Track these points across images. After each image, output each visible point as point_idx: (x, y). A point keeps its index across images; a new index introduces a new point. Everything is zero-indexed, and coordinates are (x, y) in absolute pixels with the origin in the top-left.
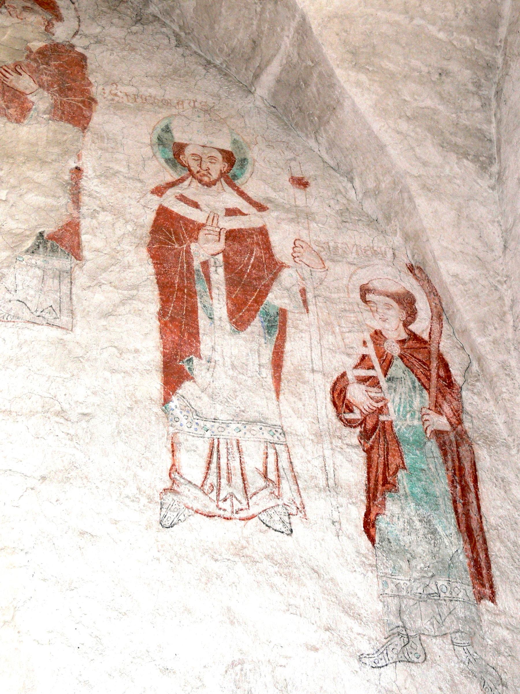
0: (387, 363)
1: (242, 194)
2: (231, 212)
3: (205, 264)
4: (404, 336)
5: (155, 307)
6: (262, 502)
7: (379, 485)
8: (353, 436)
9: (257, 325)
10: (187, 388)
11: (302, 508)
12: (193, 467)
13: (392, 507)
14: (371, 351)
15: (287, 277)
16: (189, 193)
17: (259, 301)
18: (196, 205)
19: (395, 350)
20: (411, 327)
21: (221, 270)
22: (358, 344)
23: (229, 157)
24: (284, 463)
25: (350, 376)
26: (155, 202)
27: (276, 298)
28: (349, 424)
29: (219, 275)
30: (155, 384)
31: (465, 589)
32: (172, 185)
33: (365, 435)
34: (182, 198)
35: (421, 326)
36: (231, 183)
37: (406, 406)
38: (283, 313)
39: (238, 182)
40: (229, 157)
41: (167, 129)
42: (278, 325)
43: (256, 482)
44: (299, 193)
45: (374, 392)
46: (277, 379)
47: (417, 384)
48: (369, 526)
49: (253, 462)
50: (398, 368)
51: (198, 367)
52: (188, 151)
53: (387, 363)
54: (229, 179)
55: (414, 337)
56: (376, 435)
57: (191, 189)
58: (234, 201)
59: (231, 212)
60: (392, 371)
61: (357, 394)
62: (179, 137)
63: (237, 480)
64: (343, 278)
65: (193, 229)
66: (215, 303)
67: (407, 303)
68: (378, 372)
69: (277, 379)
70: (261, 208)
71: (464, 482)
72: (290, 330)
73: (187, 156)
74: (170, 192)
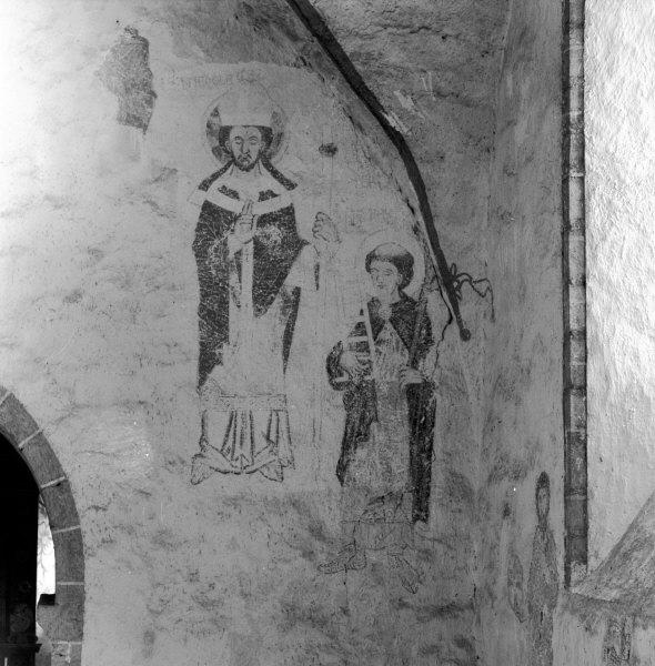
0: (377, 325)
1: (275, 173)
2: (264, 196)
3: (239, 253)
4: (398, 299)
5: (196, 303)
6: (264, 457)
7: (354, 436)
8: (339, 397)
9: (278, 301)
10: (217, 371)
11: (291, 462)
12: (216, 437)
13: (361, 453)
14: (366, 319)
15: (307, 254)
16: (230, 185)
17: (279, 283)
18: (235, 195)
19: (385, 312)
20: (404, 290)
21: (251, 258)
22: (354, 312)
23: (267, 134)
24: (283, 427)
25: (345, 345)
26: (203, 196)
27: (292, 281)
28: (337, 387)
29: (248, 265)
32: (215, 176)
33: (348, 398)
34: (224, 190)
35: (412, 290)
36: (268, 166)
37: (388, 366)
38: (297, 291)
39: (273, 161)
40: (267, 134)
41: (216, 113)
42: (293, 303)
43: (261, 442)
44: (326, 160)
46: (286, 355)
47: (401, 343)
48: (342, 468)
49: (260, 428)
50: (388, 333)
51: (225, 351)
52: (232, 135)
53: (377, 325)
54: (265, 159)
55: (405, 298)
57: (232, 179)
58: (269, 183)
59: (264, 196)
60: (382, 335)
61: (349, 360)
62: (226, 120)
63: (247, 441)
64: (350, 251)
65: (232, 218)
67: (404, 264)
68: (369, 338)
69: (286, 355)
70: (291, 186)
71: (421, 425)
72: (302, 310)
74: (217, 184)
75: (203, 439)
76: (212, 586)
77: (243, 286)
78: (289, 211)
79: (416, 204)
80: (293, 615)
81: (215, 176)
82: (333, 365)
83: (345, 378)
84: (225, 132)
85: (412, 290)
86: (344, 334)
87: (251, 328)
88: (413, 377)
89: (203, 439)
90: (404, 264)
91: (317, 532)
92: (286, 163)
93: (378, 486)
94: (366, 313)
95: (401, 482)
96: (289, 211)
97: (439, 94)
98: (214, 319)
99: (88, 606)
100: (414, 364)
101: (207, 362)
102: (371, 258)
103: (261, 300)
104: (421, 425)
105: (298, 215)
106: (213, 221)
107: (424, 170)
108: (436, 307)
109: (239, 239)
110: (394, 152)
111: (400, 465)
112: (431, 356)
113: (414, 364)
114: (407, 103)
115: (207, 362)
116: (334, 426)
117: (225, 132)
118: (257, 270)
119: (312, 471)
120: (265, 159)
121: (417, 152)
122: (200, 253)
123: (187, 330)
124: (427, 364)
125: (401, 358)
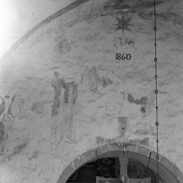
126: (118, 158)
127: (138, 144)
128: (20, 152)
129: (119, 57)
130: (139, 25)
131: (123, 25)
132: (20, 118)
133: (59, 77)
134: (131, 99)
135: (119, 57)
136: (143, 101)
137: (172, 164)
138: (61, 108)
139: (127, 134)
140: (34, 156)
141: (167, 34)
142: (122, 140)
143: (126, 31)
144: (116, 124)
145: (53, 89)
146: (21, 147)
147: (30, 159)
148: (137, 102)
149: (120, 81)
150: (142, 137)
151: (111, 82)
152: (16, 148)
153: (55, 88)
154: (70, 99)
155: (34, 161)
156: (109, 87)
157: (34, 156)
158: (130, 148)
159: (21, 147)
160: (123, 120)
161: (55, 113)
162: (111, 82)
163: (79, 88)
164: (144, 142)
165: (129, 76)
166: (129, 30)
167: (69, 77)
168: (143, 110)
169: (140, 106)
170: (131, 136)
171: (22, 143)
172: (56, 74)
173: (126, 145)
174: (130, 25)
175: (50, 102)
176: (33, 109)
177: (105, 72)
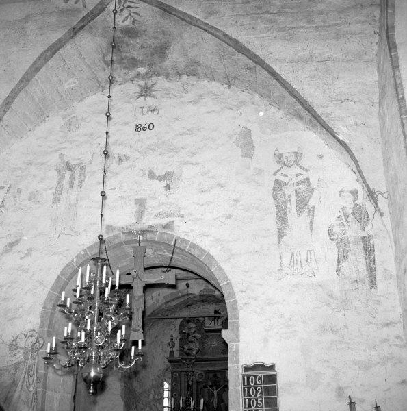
0: (347, 216)
1: (301, 167)
2: (297, 175)
5: (275, 214)
8: (334, 244)
9: (306, 211)
12: (286, 262)
14: (342, 214)
17: (306, 205)
18: (286, 176)
19: (349, 211)
20: (356, 202)
21: (294, 197)
23: (296, 155)
24: (313, 256)
25: (334, 224)
26: (274, 178)
27: (311, 203)
29: (294, 199)
30: (275, 239)
31: (368, 285)
32: (278, 171)
35: (359, 202)
37: (353, 231)
38: (313, 207)
39: (299, 163)
40: (296, 155)
42: (312, 211)
43: (304, 263)
44: (320, 161)
45: (342, 228)
46: (311, 230)
48: (338, 270)
49: (304, 257)
50: (351, 218)
51: (287, 231)
52: (284, 156)
54: (297, 163)
55: (357, 205)
56: (343, 243)
57: (285, 170)
58: (298, 170)
59: (297, 175)
60: (349, 219)
61: (337, 230)
63: (299, 263)
65: (286, 184)
66: (292, 207)
67: (355, 193)
69: (311, 230)
71: (369, 251)
72: (316, 213)
73: (284, 159)
74: (280, 172)
75: (281, 263)
76: (290, 319)
77: (292, 207)
78: (308, 179)
79: (355, 169)
80: (323, 329)
81: (278, 171)
82: (330, 232)
83: (336, 236)
84: (281, 155)
85: (359, 202)
86: (333, 220)
87: (297, 222)
88: (363, 234)
89: (281, 263)
90: (355, 193)
91: (331, 296)
92: (304, 163)
93: (354, 276)
94: (341, 212)
95: (364, 273)
96: (308, 179)
97: (357, 125)
98: (282, 218)
99: (241, 329)
100: (363, 229)
101: (281, 235)
102: (341, 192)
103: (300, 210)
104: (369, 251)
105: (311, 180)
106: (279, 186)
107: (355, 154)
108: (369, 207)
109: (289, 191)
110: (344, 151)
111: (363, 267)
112: (370, 226)
113: (363, 229)
114: (345, 130)
115: (281, 235)
116: (334, 255)
117: (281, 155)
118: (297, 200)
119: (325, 270)
120: (297, 163)
121: (352, 148)
122: (275, 198)
123: (271, 223)
124: (369, 229)
125: (358, 227)
126: (227, 329)
127: (160, 230)
128: (11, 250)
129: (139, 128)
130: (166, 89)
131: (146, 92)
132: (14, 211)
133: (66, 159)
134: (152, 176)
135: (139, 128)
136: (168, 176)
137: (205, 251)
138: (64, 194)
139: (145, 218)
140: (27, 255)
141: (201, 95)
142: (139, 227)
143: (149, 99)
144: (132, 208)
145: (56, 173)
146: (12, 245)
147: (21, 258)
148: (160, 179)
149: (138, 155)
150: (164, 221)
151: (127, 158)
152: (6, 246)
153: (59, 172)
154: (76, 182)
155: (28, 260)
156: (125, 164)
157: (27, 255)
158: (149, 236)
159: (12, 245)
160: (141, 202)
161: (56, 200)
162: (127, 158)
163: (87, 169)
164: (167, 226)
165: (151, 149)
166: (154, 96)
167: (77, 158)
168: (168, 187)
169: (164, 183)
170: (149, 221)
171: (14, 240)
172: (62, 156)
173: (143, 232)
174: (154, 91)
175: (51, 189)
176: (30, 198)
177: (121, 147)
